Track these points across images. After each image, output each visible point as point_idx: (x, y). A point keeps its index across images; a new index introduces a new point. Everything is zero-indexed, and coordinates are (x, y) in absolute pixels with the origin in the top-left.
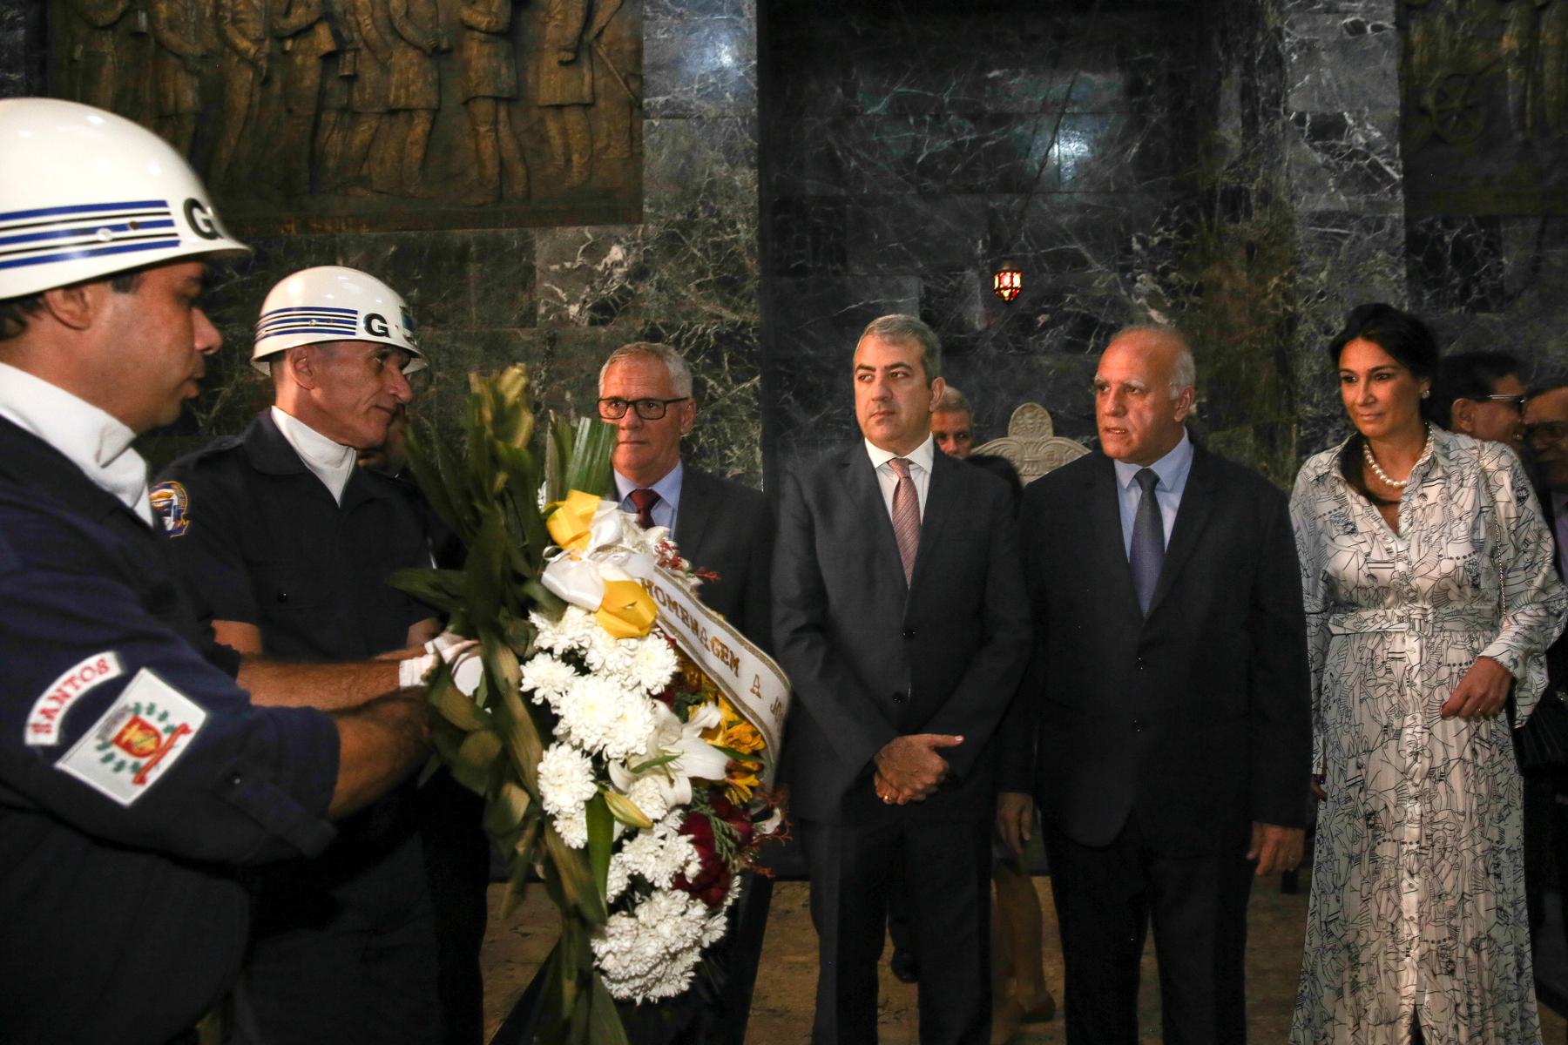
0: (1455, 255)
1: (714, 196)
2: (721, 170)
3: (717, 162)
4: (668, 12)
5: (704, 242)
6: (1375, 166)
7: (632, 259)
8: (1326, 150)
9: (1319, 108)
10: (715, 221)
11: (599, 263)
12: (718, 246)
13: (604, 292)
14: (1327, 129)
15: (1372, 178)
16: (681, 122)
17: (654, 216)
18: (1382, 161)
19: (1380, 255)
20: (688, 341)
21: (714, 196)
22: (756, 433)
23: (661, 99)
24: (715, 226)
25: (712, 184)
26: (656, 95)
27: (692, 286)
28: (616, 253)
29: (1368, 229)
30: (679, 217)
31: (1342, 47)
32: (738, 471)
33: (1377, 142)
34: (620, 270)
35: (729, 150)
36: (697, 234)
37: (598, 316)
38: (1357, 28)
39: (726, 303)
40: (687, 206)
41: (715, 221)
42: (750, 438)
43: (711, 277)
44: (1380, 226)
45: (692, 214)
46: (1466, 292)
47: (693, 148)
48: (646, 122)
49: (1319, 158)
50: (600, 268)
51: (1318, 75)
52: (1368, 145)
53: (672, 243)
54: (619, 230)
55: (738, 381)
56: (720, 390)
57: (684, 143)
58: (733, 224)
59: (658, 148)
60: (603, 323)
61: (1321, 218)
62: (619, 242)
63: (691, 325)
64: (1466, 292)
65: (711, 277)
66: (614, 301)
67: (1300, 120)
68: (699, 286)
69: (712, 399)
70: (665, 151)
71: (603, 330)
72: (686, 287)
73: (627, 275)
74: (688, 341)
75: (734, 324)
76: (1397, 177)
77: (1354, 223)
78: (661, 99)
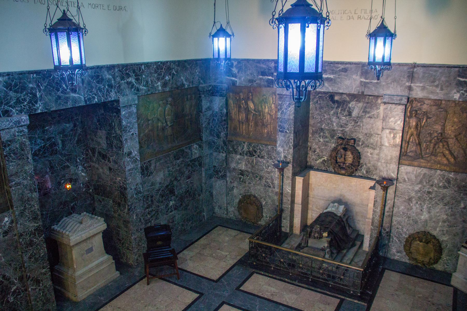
0: (146, 169)
1: (29, 201)
2: (29, 195)
3: (28, 193)
4: (12, 162)
5: (29, 212)
6: (136, 159)
7: (10, 219)
8: (129, 158)
9: (128, 151)
10: (30, 206)
11: (2, 223)
12: (32, 211)
13: (5, 229)
14: (129, 154)
15: (136, 161)
16: (19, 187)
17: (16, 210)
18: (137, 157)
19: (138, 173)
20: (29, 233)
21: (29, 201)
22: (45, 246)
23: (14, 183)
24: (30, 207)
25: (28, 199)
26: (12, 182)
27: (28, 222)
28: (6, 219)
29: (136, 170)
30: (22, 208)
31: (131, 138)
32: (42, 254)
33: (136, 154)
34: (8, 223)
35: (30, 190)
36: (27, 211)
37: (5, 235)
38: (133, 134)
39: (35, 222)
40: (24, 205)
41: (30, 206)
42: (44, 247)
43: (31, 218)
44: (137, 169)
45: (25, 206)
46: (147, 174)
47: (23, 192)
48: (11, 189)
49: (129, 159)
50: (3, 224)
51: (128, 144)
52: (135, 155)
53: (22, 214)
54: (5, 214)
55: (40, 237)
56: (37, 240)
57: (21, 191)
58: (34, 206)
59: (15, 194)
60: (6, 236)
61: (129, 170)
62: (6, 217)
63: (29, 230)
64: (147, 174)
65: (31, 218)
66: (8, 230)
67: (126, 153)
68: (29, 221)
69: (35, 243)
70: (17, 194)
71: (6, 237)
72: (27, 223)
73: (10, 223)
74: (29, 233)
75: (37, 226)
76: (139, 159)
77: (134, 169)
78: (14, 183)
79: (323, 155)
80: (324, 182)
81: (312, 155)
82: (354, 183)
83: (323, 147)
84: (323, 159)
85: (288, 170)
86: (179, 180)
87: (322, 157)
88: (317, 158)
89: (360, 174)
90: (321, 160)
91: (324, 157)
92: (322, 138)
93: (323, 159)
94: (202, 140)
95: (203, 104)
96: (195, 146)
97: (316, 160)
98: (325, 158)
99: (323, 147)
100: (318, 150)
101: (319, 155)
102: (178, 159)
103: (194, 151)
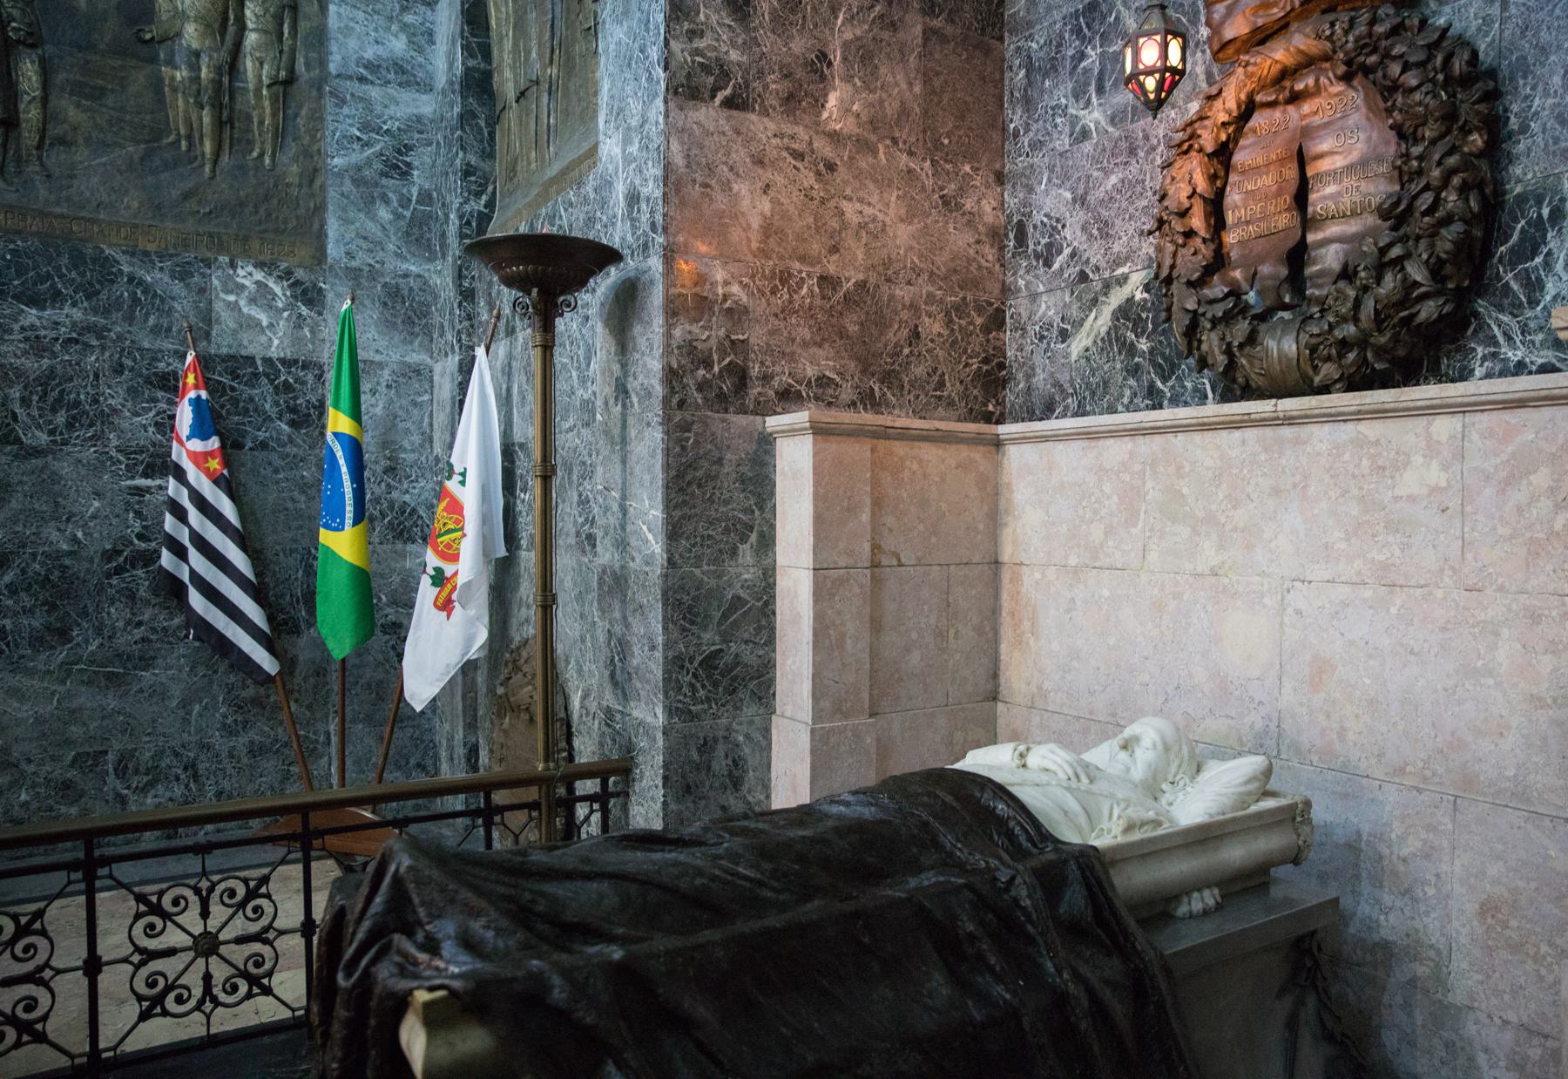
79: (1118, 263)
80: (1109, 532)
81: (1034, 297)
82: (1436, 476)
83: (1114, 179)
84: (1117, 298)
85: (649, 323)
86: (38, 452)
87: (1107, 287)
88: (1074, 312)
89: (1514, 356)
90: (1100, 321)
91: (1122, 281)
92: (1100, 90)
93: (1117, 298)
94: (321, 255)
95: (333, 22)
96: (248, 275)
97: (1064, 336)
98: (1135, 285)
99: (1114, 179)
100: (1072, 234)
101: (1083, 277)
102: (36, 302)
103: (235, 307)
